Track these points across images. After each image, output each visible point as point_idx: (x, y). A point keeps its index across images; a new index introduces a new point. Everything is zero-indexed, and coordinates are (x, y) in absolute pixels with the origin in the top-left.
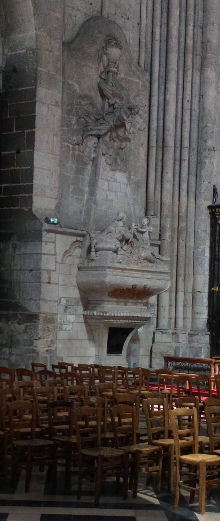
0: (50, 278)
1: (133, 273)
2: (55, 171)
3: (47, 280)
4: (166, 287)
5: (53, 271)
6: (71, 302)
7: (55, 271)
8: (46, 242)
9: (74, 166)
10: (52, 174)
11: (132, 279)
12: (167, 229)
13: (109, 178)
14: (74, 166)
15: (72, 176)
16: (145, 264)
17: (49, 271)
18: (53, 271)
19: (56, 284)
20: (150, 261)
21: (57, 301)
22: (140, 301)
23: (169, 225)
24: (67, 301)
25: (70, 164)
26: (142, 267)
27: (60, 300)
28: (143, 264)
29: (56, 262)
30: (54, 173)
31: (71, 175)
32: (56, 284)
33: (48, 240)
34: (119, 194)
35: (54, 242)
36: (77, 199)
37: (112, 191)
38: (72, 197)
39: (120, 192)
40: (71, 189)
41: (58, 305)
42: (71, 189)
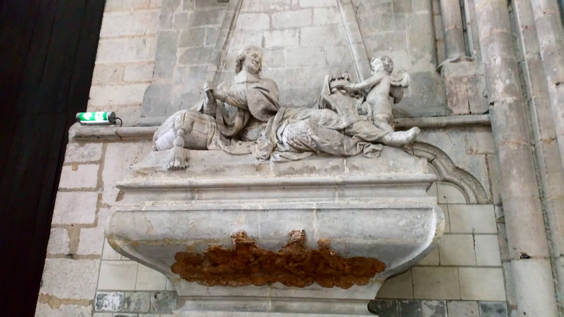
0: (75, 243)
1: (231, 200)
2: (151, 35)
3: (66, 250)
4: (423, 236)
5: (88, 226)
6: (139, 302)
7: (95, 225)
8: (75, 165)
9: (190, 12)
10: (144, 42)
11: (227, 217)
12: (496, 71)
13: (272, 7)
14: (190, 12)
15: (181, 31)
16: (298, 165)
17: (74, 230)
18: (88, 226)
19: (93, 257)
20: (317, 151)
21: (92, 302)
22: (338, 292)
23: (499, 61)
24: (128, 301)
25: (180, 10)
26: (280, 175)
27: (101, 297)
28: (284, 167)
29: (99, 205)
30: (149, 39)
31: (180, 30)
32: (93, 257)
33: (81, 160)
34: (306, 32)
35: (101, 162)
36: (195, 69)
37: (282, 30)
38: (180, 69)
39: (312, 25)
40: (178, 55)
41: (93, 311)
42: (178, 55)
